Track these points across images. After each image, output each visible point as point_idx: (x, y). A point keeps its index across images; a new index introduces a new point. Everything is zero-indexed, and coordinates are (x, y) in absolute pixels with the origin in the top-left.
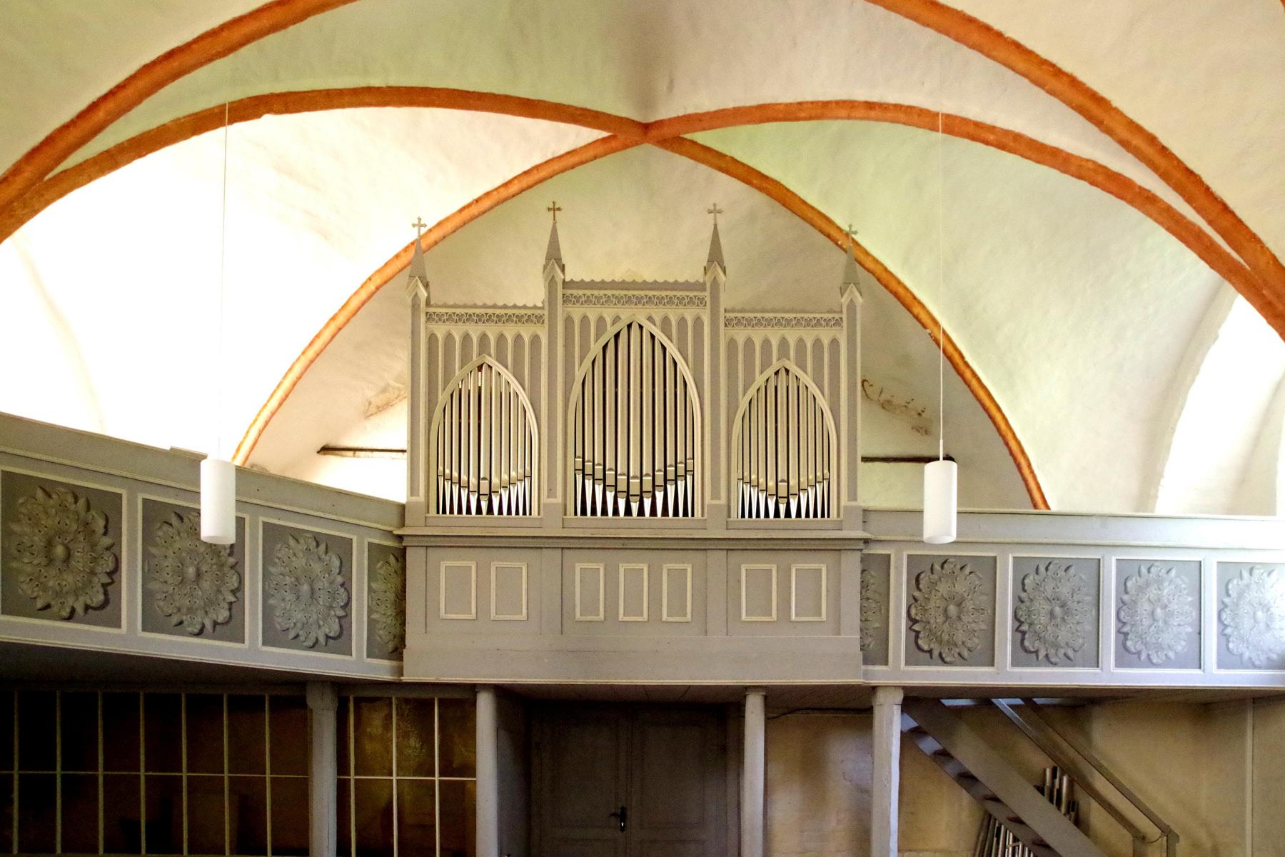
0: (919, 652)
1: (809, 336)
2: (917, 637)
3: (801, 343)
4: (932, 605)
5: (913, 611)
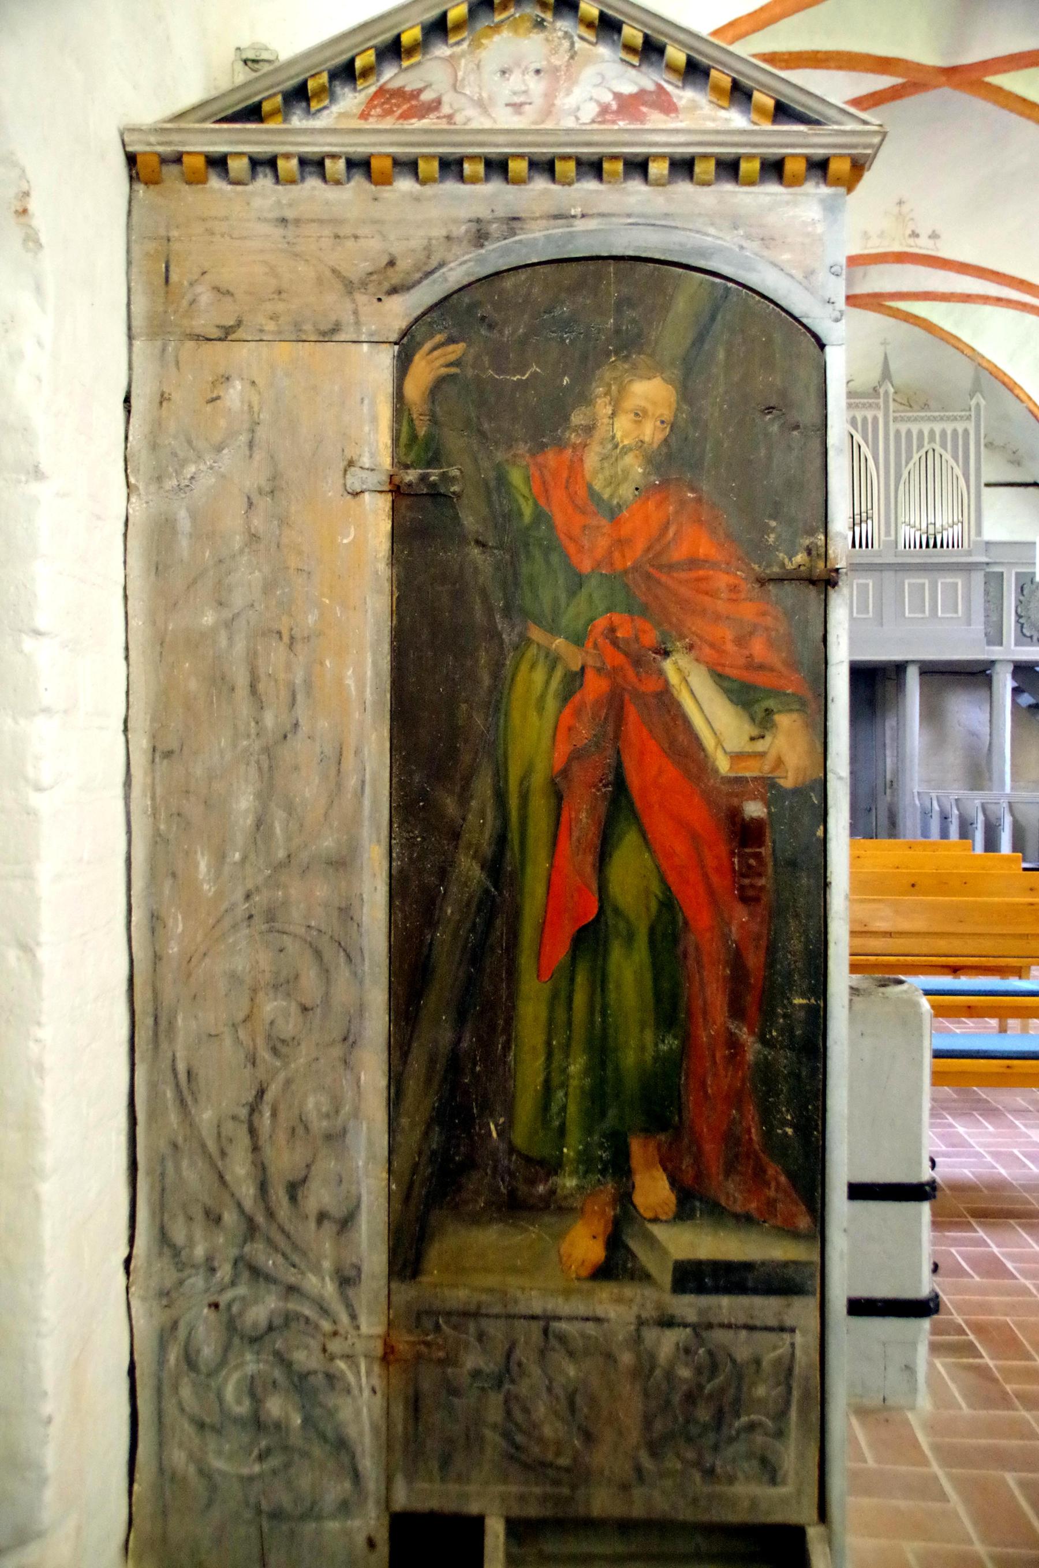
0: (1023, 637)
1: (949, 427)
2: (1022, 627)
3: (943, 433)
4: (1032, 605)
5: (1019, 610)
